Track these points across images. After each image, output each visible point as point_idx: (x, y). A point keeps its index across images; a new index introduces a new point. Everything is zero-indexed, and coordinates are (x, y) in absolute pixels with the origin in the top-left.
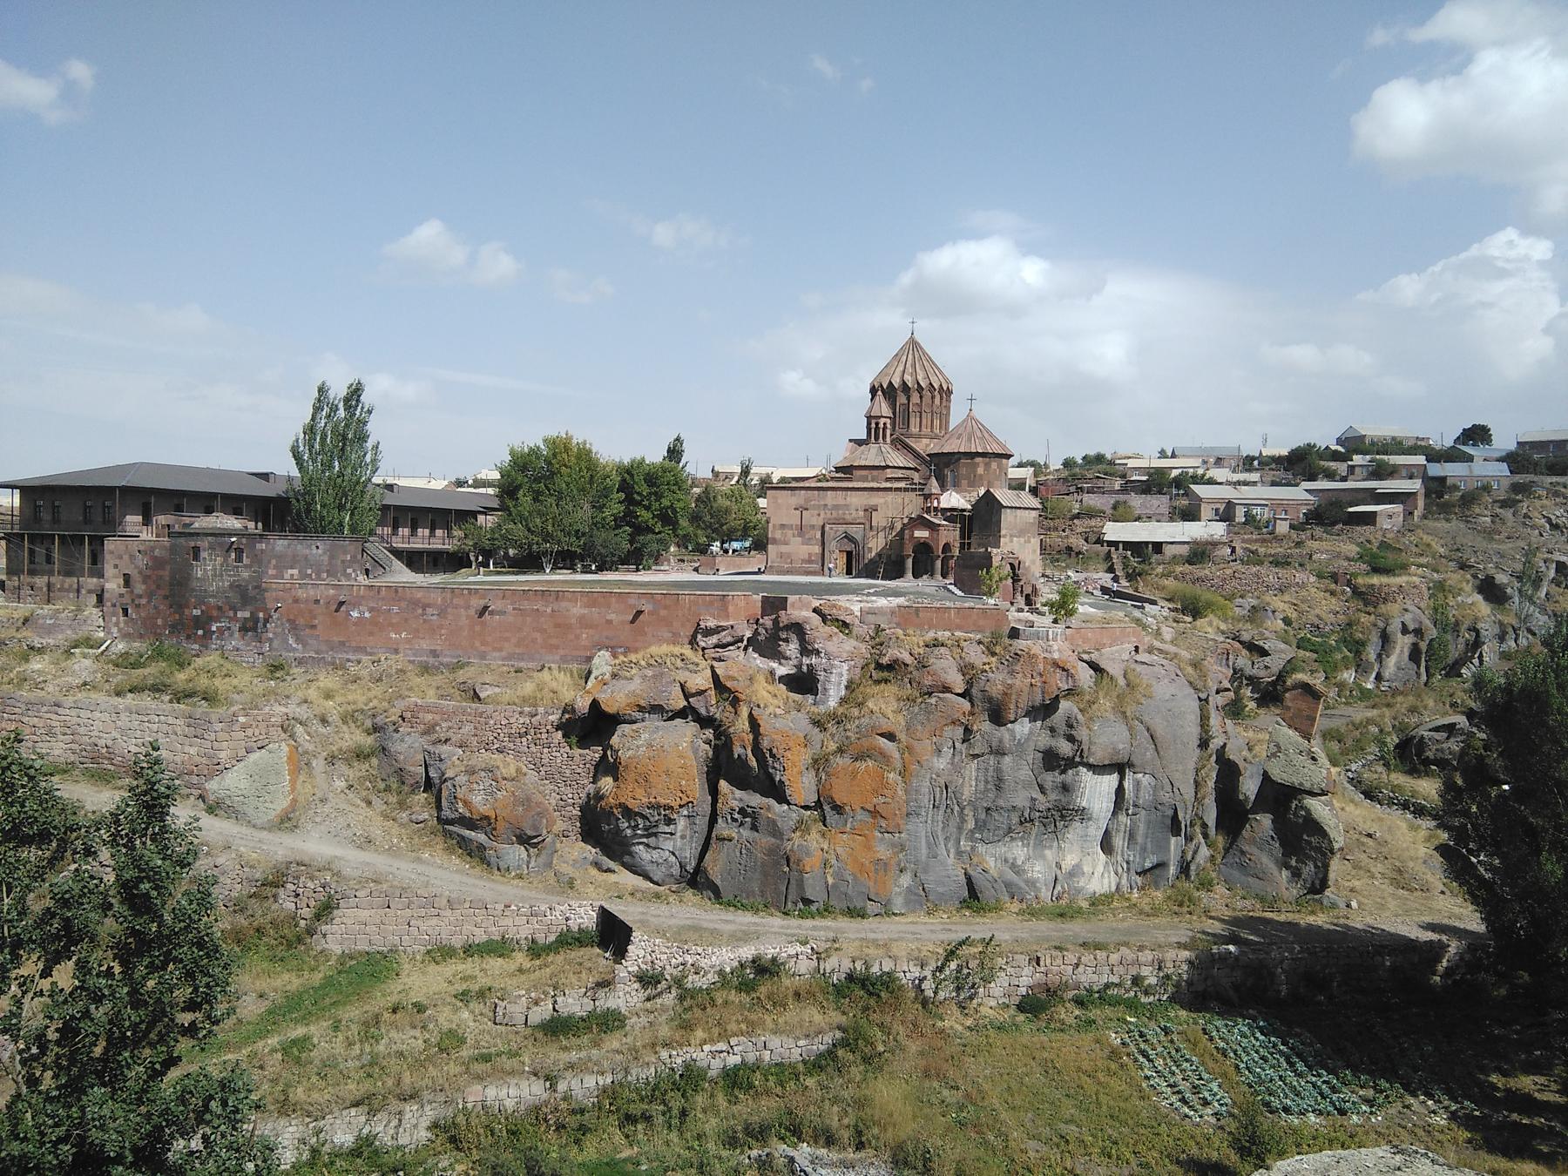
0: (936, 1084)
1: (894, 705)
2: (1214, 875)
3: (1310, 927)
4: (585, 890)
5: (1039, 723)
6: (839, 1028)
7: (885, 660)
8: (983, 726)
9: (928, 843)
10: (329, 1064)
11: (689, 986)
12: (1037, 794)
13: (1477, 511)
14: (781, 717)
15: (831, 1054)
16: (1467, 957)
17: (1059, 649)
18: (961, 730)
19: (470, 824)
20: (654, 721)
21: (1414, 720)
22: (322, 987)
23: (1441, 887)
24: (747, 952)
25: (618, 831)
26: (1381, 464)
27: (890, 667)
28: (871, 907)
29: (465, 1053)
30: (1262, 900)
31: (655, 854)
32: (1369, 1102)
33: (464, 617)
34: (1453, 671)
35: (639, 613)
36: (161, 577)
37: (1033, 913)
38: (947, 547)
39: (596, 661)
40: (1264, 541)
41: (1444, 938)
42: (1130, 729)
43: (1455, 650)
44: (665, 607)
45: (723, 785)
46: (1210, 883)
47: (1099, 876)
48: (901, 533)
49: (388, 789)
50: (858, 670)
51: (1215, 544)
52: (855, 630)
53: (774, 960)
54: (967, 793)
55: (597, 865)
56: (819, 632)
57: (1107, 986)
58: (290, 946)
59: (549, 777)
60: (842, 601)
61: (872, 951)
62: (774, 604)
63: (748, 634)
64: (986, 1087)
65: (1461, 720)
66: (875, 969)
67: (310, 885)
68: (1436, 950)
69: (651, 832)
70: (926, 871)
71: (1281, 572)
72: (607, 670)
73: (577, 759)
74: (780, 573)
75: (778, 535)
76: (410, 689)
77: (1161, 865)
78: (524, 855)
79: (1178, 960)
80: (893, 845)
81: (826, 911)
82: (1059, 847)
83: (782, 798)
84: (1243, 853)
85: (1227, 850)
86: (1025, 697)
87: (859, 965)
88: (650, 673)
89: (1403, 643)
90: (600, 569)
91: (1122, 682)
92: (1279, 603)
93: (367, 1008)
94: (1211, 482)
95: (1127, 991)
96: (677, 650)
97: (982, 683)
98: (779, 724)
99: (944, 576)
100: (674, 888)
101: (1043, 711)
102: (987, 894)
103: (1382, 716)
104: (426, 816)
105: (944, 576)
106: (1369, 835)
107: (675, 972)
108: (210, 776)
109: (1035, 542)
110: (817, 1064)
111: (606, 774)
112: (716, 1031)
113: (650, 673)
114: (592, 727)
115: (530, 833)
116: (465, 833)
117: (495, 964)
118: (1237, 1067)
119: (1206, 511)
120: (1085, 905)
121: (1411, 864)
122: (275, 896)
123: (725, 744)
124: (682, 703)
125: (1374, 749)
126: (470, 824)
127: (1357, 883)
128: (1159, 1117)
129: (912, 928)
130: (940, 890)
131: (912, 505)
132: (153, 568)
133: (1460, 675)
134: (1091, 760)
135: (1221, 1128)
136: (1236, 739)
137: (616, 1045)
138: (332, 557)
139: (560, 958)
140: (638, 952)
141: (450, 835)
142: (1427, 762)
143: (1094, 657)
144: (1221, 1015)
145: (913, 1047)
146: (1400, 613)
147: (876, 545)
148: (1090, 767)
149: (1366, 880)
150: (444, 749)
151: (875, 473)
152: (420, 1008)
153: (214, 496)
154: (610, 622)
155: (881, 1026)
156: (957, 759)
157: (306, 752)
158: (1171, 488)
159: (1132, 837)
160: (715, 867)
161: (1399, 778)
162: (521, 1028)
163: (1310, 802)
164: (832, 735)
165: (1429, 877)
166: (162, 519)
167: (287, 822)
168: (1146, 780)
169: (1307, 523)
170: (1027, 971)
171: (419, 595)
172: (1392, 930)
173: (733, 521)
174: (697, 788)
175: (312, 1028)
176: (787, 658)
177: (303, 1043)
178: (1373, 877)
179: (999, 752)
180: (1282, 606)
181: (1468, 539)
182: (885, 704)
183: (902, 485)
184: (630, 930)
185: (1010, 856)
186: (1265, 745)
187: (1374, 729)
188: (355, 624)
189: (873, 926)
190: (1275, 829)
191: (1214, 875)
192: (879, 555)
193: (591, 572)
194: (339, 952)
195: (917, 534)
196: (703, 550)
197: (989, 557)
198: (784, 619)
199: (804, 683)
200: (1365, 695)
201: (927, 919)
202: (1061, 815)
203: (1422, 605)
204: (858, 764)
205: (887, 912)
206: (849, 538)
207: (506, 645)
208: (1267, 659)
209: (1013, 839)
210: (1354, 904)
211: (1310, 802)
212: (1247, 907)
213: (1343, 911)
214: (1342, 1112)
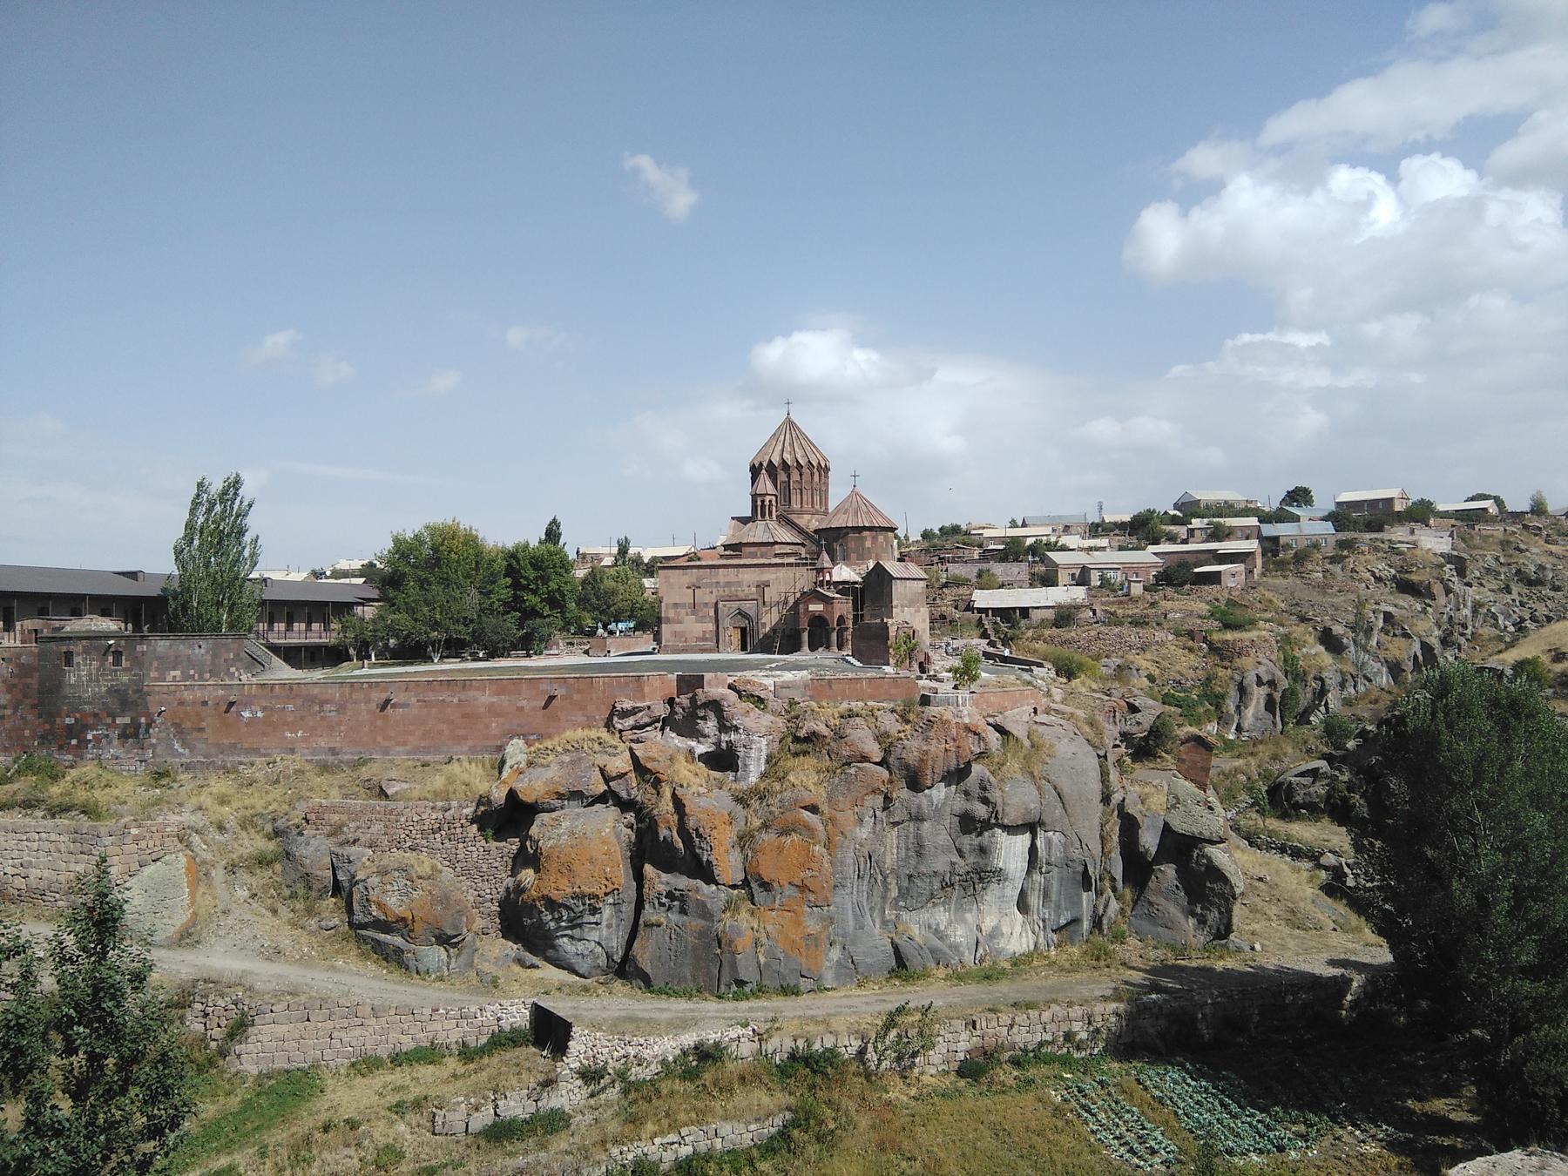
0: (892, 1156)
5: (953, 787)
7: (802, 733)
8: (902, 793)
9: (855, 915)
12: (956, 858)
14: (707, 797)
17: (969, 714)
18: (881, 798)
20: (574, 808)
21: (1276, 767)
23: (1332, 925)
26: (1218, 527)
28: (804, 984)
30: (1173, 949)
32: (1305, 1138)
34: (1303, 719)
35: (552, 698)
36: (27, 686)
37: (960, 978)
38: (841, 620)
39: (509, 749)
40: (1121, 603)
41: (1347, 973)
42: (1039, 788)
43: (1305, 698)
44: (579, 691)
45: (648, 869)
47: (1018, 936)
50: (776, 745)
51: (1078, 607)
52: (770, 705)
54: (890, 861)
56: (737, 709)
57: (1041, 1044)
59: (465, 873)
61: (811, 1028)
62: (690, 683)
64: (942, 1155)
66: (817, 1046)
70: (854, 943)
71: (1142, 632)
73: (494, 852)
76: (311, 789)
77: (1075, 921)
79: (1108, 1012)
80: (822, 919)
81: (761, 991)
83: (710, 878)
84: (1151, 904)
85: (1135, 902)
89: (1259, 694)
91: (1027, 743)
92: (1143, 662)
94: (1064, 549)
95: (1060, 1048)
96: (594, 734)
98: (703, 802)
101: (957, 775)
102: (914, 962)
106: (1260, 879)
111: (526, 865)
113: (567, 758)
114: (510, 818)
119: (1063, 577)
120: (1007, 965)
123: (649, 827)
124: (603, 788)
125: (1244, 797)
127: (1257, 926)
129: (845, 1001)
130: (869, 961)
132: (19, 676)
133: (1309, 722)
138: (215, 656)
142: (1297, 806)
143: (999, 720)
149: (1264, 923)
150: (353, 851)
153: (82, 597)
156: (879, 827)
159: (1046, 895)
161: (1274, 824)
163: (1211, 850)
164: (756, 811)
166: (29, 624)
168: (1056, 837)
170: (964, 1036)
171: (316, 691)
174: (622, 875)
178: (1270, 919)
179: (918, 818)
180: (1144, 664)
181: (1306, 595)
182: (806, 777)
185: (932, 921)
186: (1158, 795)
187: (1243, 778)
188: (247, 725)
198: (701, 697)
199: (723, 760)
200: (1229, 746)
201: (858, 992)
202: (981, 876)
203: (1274, 658)
204: (783, 839)
205: (820, 989)
207: (411, 738)
209: (935, 905)
210: (1258, 947)
211: (1211, 850)
212: (1157, 955)
213: (1250, 955)
214: (1281, 1149)
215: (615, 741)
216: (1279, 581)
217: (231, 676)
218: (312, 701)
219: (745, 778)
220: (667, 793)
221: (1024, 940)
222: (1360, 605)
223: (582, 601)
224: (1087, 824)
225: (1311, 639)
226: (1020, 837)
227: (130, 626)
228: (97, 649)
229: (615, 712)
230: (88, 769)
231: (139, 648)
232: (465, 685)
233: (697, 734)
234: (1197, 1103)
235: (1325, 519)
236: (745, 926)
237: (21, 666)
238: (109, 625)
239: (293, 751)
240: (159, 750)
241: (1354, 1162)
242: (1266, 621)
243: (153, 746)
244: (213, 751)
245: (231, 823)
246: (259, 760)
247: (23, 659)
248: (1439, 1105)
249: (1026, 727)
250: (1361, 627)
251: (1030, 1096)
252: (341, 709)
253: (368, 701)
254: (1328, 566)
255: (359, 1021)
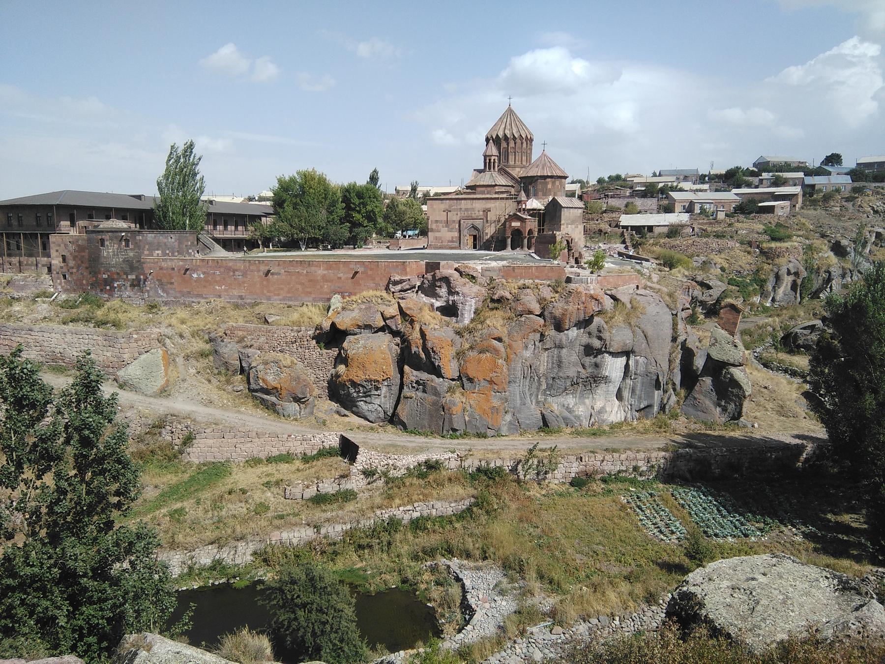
0: (526, 525)
1: (501, 322)
2: (679, 411)
3: (731, 438)
4: (332, 426)
5: (582, 330)
6: (473, 496)
7: (496, 297)
8: (551, 332)
10: (195, 523)
11: (391, 476)
12: (581, 369)
13: (832, 204)
15: (469, 510)
16: (817, 452)
17: (594, 288)
18: (539, 335)
19: (267, 392)
20: (366, 334)
22: (189, 481)
23: (805, 415)
24: (422, 458)
25: (349, 394)
27: (498, 301)
29: (270, 514)
30: (705, 424)
31: (370, 406)
33: (257, 276)
34: (815, 295)
35: (356, 273)
37: (578, 433)
39: (333, 300)
40: (711, 223)
42: (633, 332)
43: (817, 283)
45: (407, 368)
46: (677, 415)
47: (615, 413)
48: (504, 224)
49: (219, 373)
51: (683, 226)
52: (479, 280)
53: (437, 462)
54: (542, 370)
55: (338, 413)
57: (619, 472)
58: (170, 460)
59: (310, 365)
60: (471, 263)
61: (490, 456)
62: (432, 267)
63: (418, 284)
65: (818, 323)
66: (492, 465)
67: (179, 426)
68: (800, 449)
69: (367, 394)
70: (519, 412)
72: (339, 305)
73: (325, 355)
74: (436, 248)
75: (434, 226)
76: (229, 318)
77: (649, 406)
78: (298, 408)
79: (659, 458)
81: (465, 435)
82: (593, 397)
83: (439, 375)
84: (695, 398)
85: (686, 398)
86: (574, 314)
87: (483, 463)
88: (364, 307)
90: (333, 248)
91: (629, 306)
92: (719, 259)
93: (214, 492)
94: (681, 190)
95: (630, 474)
96: (378, 293)
97: (550, 309)
99: (529, 248)
100: (381, 424)
101: (584, 323)
102: (553, 424)
103: (774, 321)
104: (242, 388)
105: (529, 248)
106: (766, 388)
107: (383, 469)
108: (119, 368)
109: (581, 228)
110: (461, 516)
111: (341, 363)
112: (406, 499)
113: (364, 307)
114: (333, 337)
115: (300, 396)
116: (263, 396)
117: (284, 467)
118: (690, 513)
119: (678, 207)
120: (607, 428)
121: (788, 403)
122: (160, 433)
125: (769, 339)
126: (267, 392)
127: (758, 414)
128: (647, 540)
129: (512, 443)
130: (528, 422)
131: (510, 207)
133: (819, 298)
134: (611, 350)
135: (681, 545)
136: (692, 336)
137: (352, 508)
139: (320, 463)
140: (362, 458)
141: (256, 398)
142: (799, 347)
143: (613, 292)
144: (681, 486)
145: (514, 506)
146: (786, 263)
147: (490, 231)
148: (610, 353)
149: (763, 412)
151: (489, 189)
152: (244, 492)
154: (340, 278)
155: (496, 495)
157: (172, 354)
158: (657, 193)
159: (633, 391)
160: (404, 413)
161: (782, 356)
162: (300, 501)
163: (733, 370)
165: (798, 409)
167: (164, 392)
168: (641, 360)
169: (735, 213)
170: (575, 464)
172: (777, 439)
173: (408, 219)
174: (392, 370)
175: (185, 503)
176: (440, 297)
177: (181, 511)
178: (767, 410)
179: (560, 347)
180: (720, 260)
181: (826, 220)
182: (496, 322)
183: (505, 196)
184: (358, 447)
185: (566, 403)
186: (709, 339)
187: (770, 329)
189: (491, 442)
190: (714, 385)
191: (679, 411)
192: (492, 237)
193: (328, 250)
194: (197, 462)
195: (514, 224)
196: (391, 236)
197: (554, 237)
198: (438, 275)
199: (450, 310)
200: (765, 310)
202: (595, 379)
204: (481, 355)
206: (474, 227)
208: (711, 291)
209: (567, 394)
210: (756, 425)
211: (733, 370)
212: (698, 428)
213: (750, 429)
214: (746, 536)
215: (390, 298)
216: (811, 212)
217: (190, 254)
218: (229, 269)
219: (462, 321)
220: (418, 329)
221: (619, 415)
222: (862, 227)
223: (386, 218)
224: (661, 352)
225: (825, 248)
226: (619, 359)
227: (138, 225)
228: (116, 237)
229: (391, 283)
230: (115, 302)
231: (138, 238)
232: (310, 264)
233: (436, 296)
234: (704, 508)
235: (846, 174)
236: (459, 402)
237: (79, 246)
238: (122, 224)
239: (220, 297)
240: (151, 293)
241: (788, 545)
242: (798, 236)
243: (148, 291)
244: (178, 295)
245: (187, 334)
246: (202, 301)
247: (80, 242)
248: (846, 518)
249: (630, 297)
250: (860, 242)
251: (609, 499)
252: (244, 275)
253: (259, 271)
254: (844, 203)
255: (250, 440)
